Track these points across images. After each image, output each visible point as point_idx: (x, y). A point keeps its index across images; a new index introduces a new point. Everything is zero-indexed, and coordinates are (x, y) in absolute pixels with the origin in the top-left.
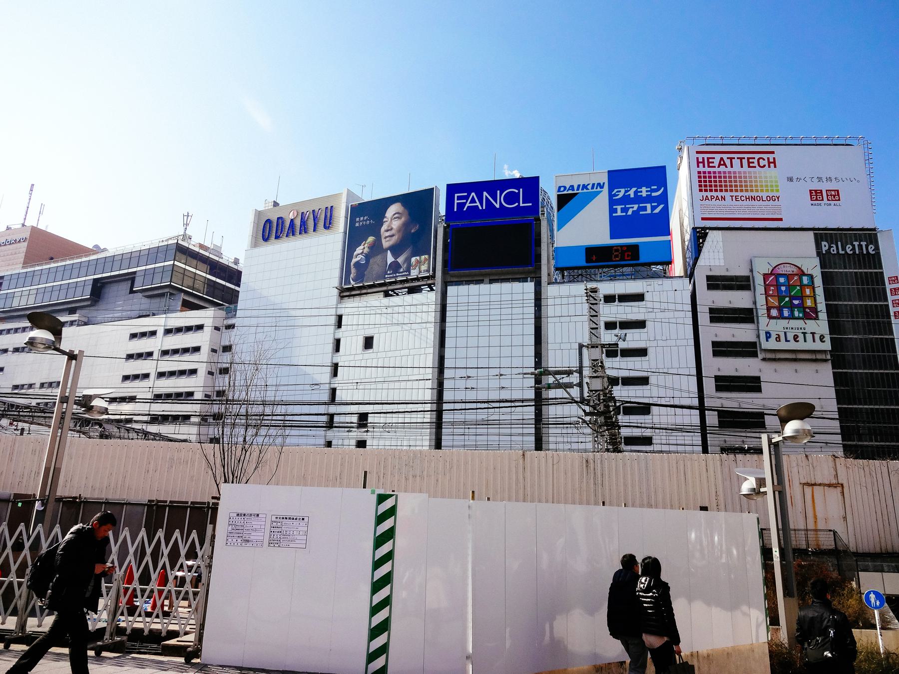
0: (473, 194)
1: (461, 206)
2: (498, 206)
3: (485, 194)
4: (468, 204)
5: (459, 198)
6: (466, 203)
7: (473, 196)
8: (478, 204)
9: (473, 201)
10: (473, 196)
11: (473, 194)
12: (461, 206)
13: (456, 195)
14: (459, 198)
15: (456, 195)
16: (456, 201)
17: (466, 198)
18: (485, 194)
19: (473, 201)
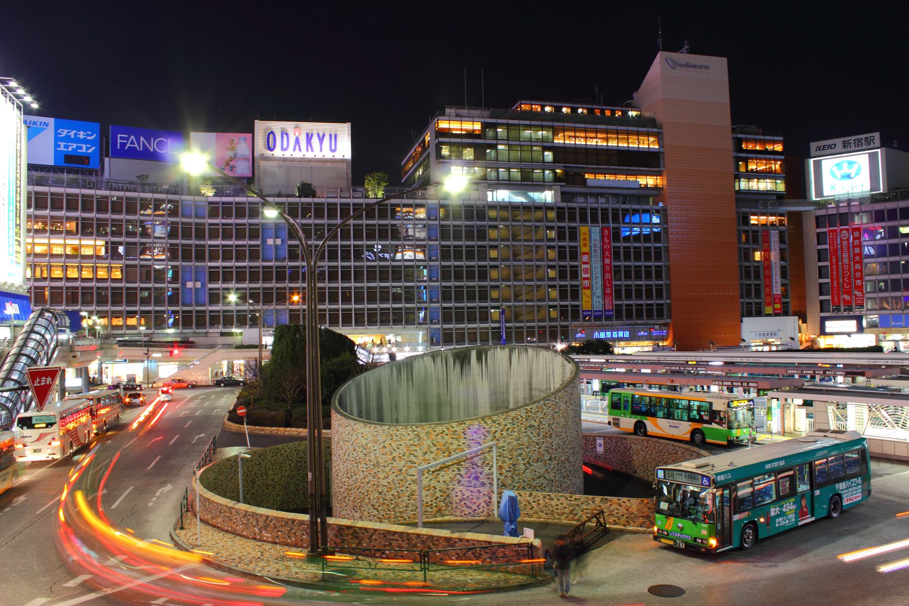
0: (132, 137)
1: (123, 145)
2: (152, 150)
3: (142, 138)
4: (128, 145)
5: (121, 138)
6: (126, 144)
7: (132, 139)
8: (136, 146)
9: (132, 143)
10: (132, 139)
11: (132, 137)
12: (123, 145)
13: (119, 135)
14: (121, 138)
15: (119, 135)
16: (119, 141)
17: (127, 139)
18: (142, 138)
19: (132, 143)
